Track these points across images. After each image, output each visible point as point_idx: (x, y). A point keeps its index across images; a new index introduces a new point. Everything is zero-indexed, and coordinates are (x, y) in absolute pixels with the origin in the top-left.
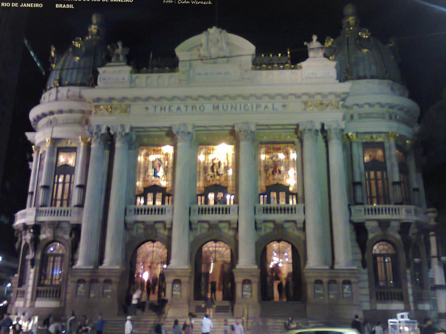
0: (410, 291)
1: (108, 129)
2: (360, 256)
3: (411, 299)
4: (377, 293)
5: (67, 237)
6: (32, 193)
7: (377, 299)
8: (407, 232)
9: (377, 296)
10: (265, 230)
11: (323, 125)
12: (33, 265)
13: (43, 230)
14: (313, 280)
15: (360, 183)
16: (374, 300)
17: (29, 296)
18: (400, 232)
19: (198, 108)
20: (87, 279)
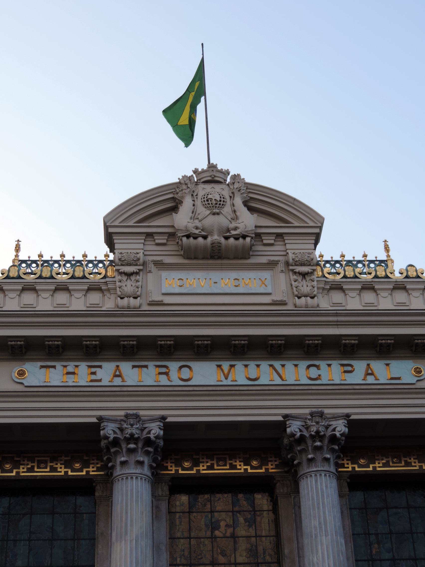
19: (174, 374)
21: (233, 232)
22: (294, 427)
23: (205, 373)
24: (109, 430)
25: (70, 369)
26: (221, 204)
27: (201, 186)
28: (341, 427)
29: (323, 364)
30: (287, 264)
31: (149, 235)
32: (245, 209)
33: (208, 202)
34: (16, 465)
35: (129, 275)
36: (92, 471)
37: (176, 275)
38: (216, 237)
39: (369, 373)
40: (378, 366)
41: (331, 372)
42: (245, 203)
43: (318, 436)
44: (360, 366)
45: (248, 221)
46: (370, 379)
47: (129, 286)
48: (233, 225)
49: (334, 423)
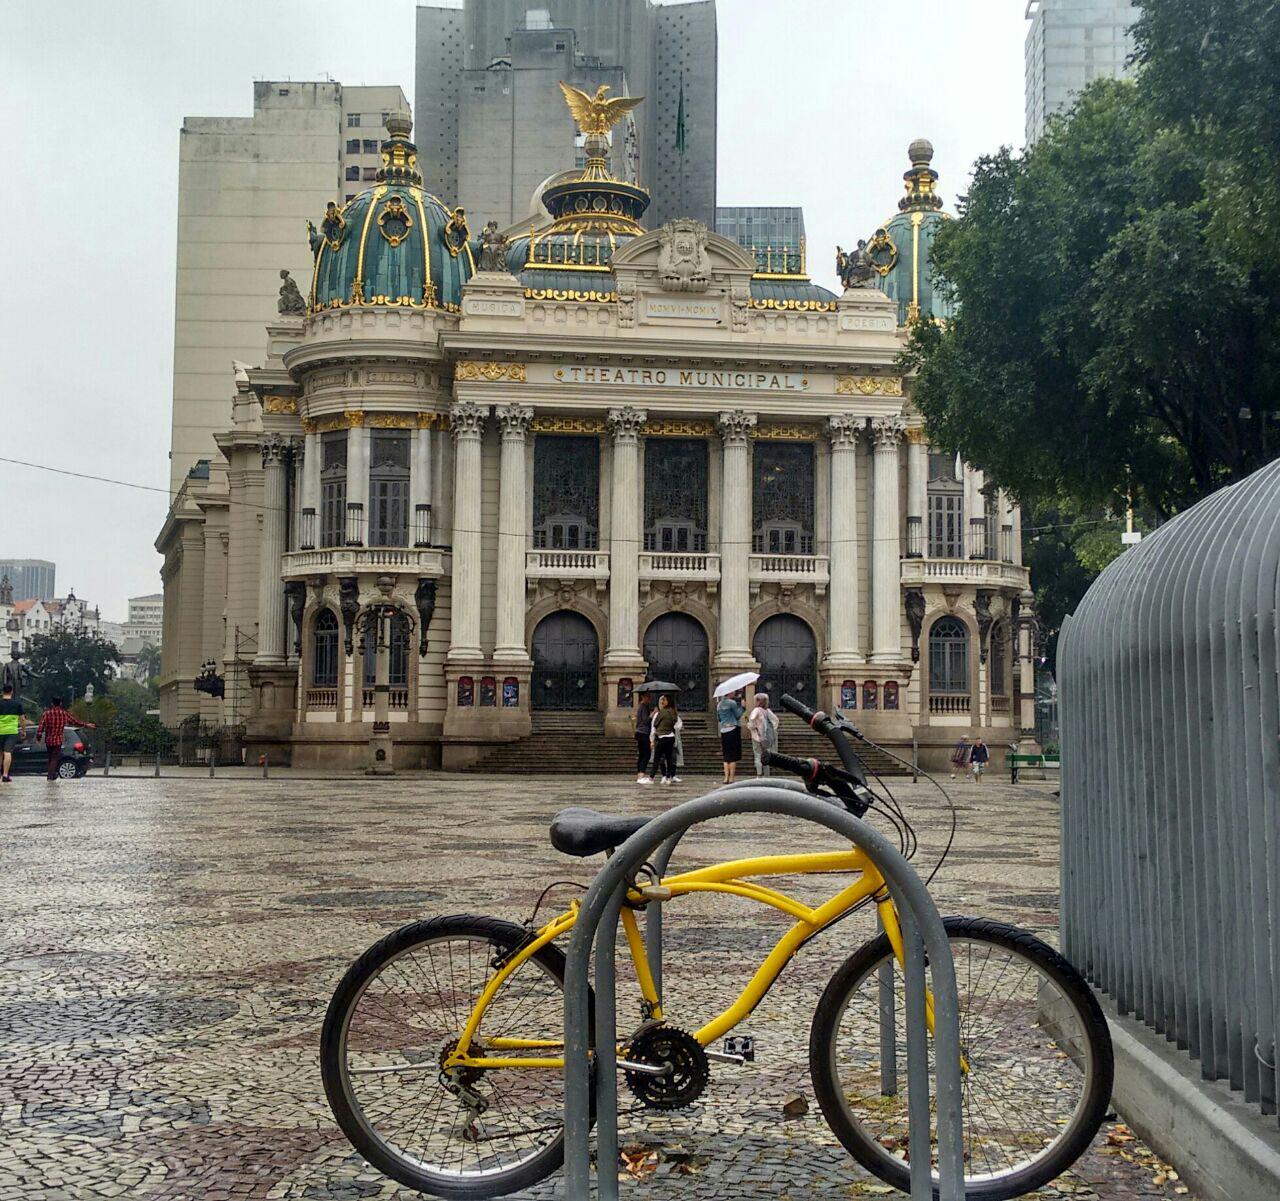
0: (983, 698)
1: (493, 409)
2: (909, 643)
3: (983, 709)
4: (931, 700)
5: (411, 601)
6: (312, 512)
7: (931, 709)
8: (987, 605)
9: (931, 704)
10: (761, 599)
11: (869, 420)
12: (350, 652)
13: (362, 588)
14: (841, 681)
15: (919, 520)
16: (927, 710)
17: (349, 703)
18: (975, 605)
19: (654, 377)
20: (475, 677)
21: (697, 276)
22: (725, 419)
23: (673, 378)
24: (614, 416)
25: (590, 371)
26: (688, 251)
27: (677, 234)
28: (753, 421)
29: (746, 375)
30: (730, 297)
31: (641, 272)
32: (705, 253)
33: (683, 251)
34: (553, 424)
35: (627, 303)
36: (598, 429)
37: (657, 302)
38: (685, 279)
39: (775, 381)
40: (781, 378)
41: (751, 381)
42: (706, 249)
43: (739, 425)
44: (769, 377)
45: (707, 264)
46: (775, 387)
47: (626, 311)
48: (698, 270)
49: (749, 417)
